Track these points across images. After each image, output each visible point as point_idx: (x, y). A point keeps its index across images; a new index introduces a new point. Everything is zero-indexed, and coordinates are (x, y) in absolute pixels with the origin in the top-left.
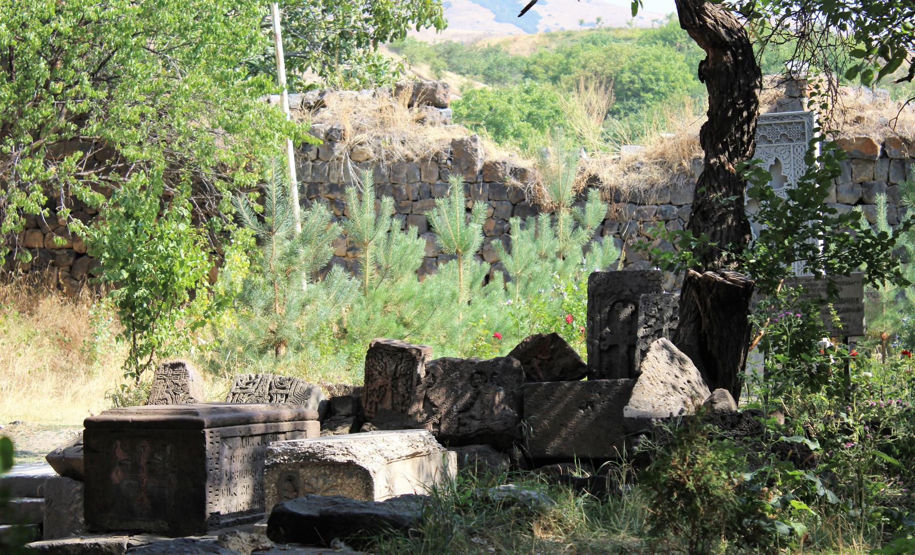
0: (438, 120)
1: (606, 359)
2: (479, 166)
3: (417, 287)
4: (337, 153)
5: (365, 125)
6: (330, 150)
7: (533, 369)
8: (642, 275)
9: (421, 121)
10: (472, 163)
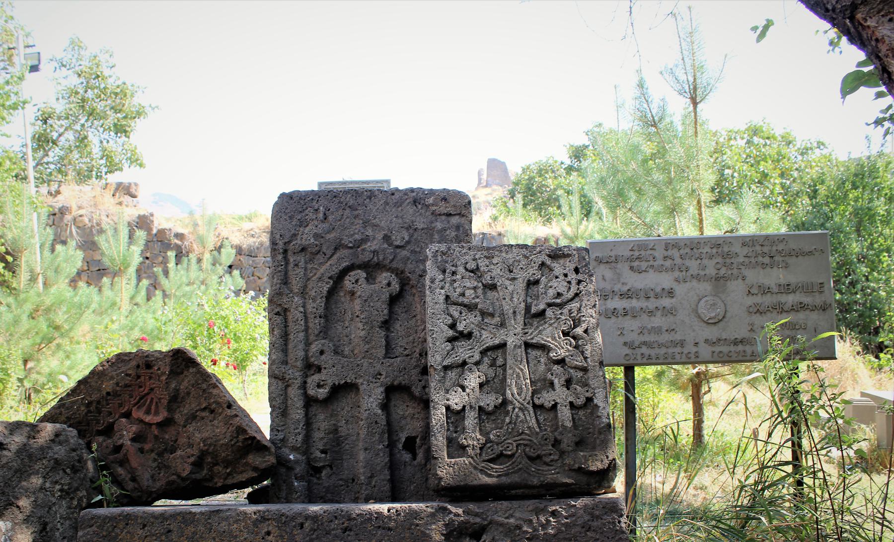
0: (130, 204)
1: (322, 422)
2: (155, 231)
3: (68, 293)
4: (65, 221)
5: (85, 204)
6: (62, 219)
7: (118, 449)
8: (415, 202)
9: (120, 204)
10: (151, 229)
